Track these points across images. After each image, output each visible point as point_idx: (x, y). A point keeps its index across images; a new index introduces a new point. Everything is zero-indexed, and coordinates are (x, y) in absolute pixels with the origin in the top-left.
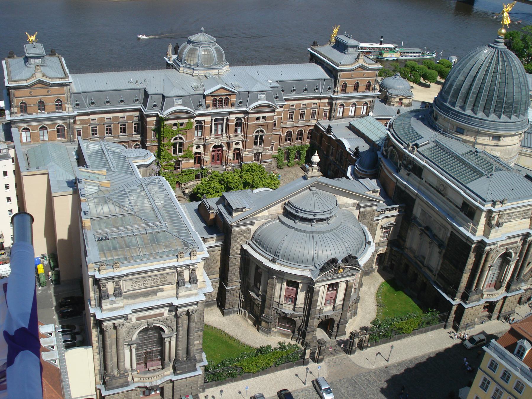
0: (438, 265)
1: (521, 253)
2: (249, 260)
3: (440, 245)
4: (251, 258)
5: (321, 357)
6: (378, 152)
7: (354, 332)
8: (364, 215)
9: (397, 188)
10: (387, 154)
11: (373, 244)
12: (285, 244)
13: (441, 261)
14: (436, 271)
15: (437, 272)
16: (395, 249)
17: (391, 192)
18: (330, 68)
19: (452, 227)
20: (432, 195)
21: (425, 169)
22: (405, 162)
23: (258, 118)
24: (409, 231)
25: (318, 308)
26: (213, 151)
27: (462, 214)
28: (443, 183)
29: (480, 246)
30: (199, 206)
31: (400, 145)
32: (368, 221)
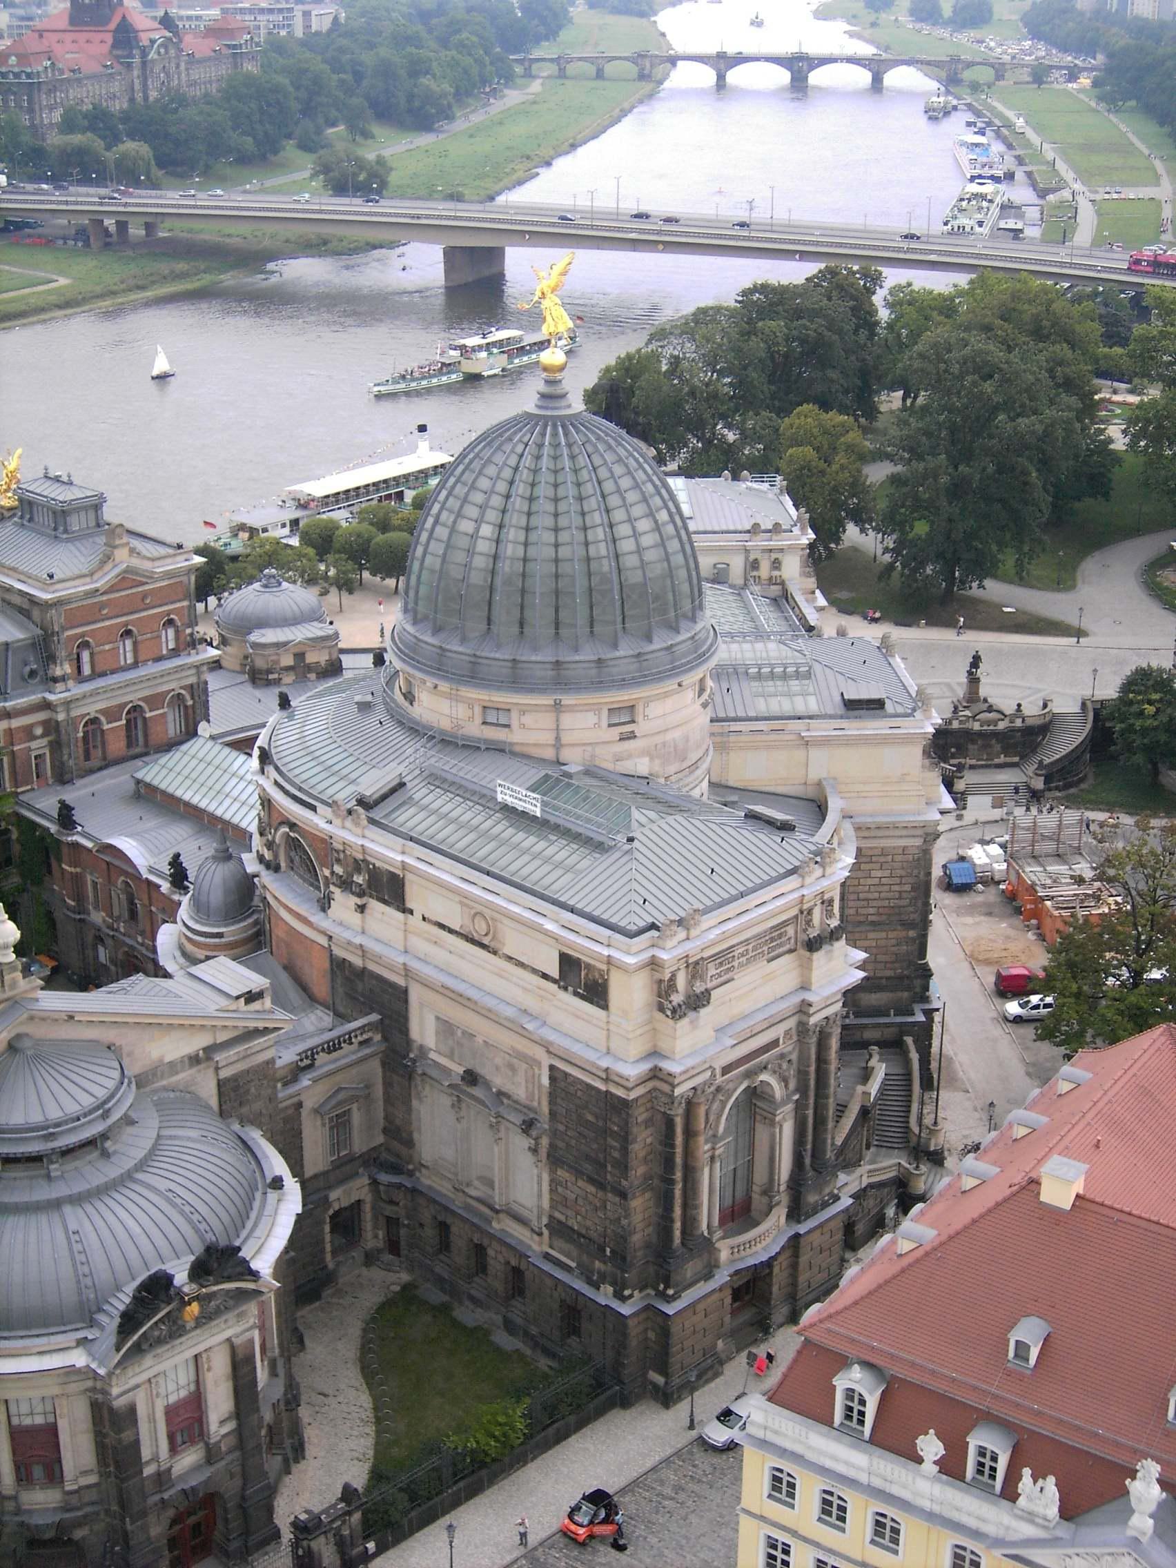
0: (540, 1196)
1: (802, 1074)
3: (528, 1126)
6: (245, 856)
7: (303, 1517)
9: (339, 966)
10: (276, 856)
11: (292, 1187)
13: (546, 1177)
14: (539, 1218)
15: (545, 1221)
16: (384, 1178)
17: (321, 987)
18: (17, 600)
19: (549, 1052)
21: (409, 877)
22: (338, 869)
24: (415, 1103)
25: (148, 1471)
27: (568, 999)
28: (480, 908)
29: (655, 1089)
31: (308, 814)
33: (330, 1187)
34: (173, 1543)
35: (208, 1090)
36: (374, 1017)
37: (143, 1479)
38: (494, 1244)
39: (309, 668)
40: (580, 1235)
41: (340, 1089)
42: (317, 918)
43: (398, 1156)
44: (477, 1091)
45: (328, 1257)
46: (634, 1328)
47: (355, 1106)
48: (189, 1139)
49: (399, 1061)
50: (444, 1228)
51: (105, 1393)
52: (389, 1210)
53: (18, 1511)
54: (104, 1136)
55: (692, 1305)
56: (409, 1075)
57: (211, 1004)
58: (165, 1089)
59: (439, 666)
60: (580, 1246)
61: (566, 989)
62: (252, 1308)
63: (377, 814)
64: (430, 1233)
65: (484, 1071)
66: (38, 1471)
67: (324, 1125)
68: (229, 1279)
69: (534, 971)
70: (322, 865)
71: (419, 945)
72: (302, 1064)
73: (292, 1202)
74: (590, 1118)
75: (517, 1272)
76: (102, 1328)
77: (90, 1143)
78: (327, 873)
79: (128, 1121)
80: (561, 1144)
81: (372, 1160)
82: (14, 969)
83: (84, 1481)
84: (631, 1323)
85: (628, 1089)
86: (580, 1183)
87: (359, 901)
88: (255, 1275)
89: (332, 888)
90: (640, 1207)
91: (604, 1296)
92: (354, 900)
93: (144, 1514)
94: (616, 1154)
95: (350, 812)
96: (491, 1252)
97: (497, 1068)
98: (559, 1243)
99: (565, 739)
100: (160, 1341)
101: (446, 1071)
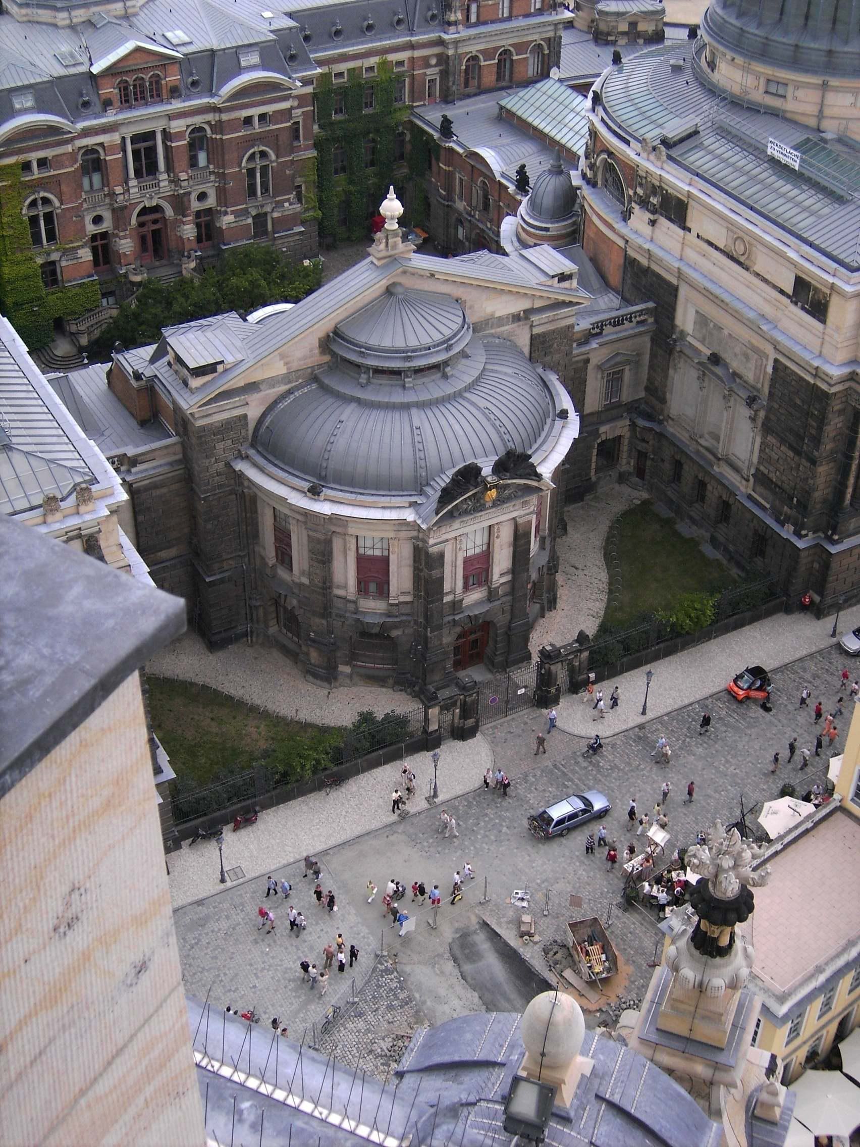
0: (752, 452)
2: (254, 499)
3: (751, 401)
4: (259, 494)
5: (470, 722)
6: (573, 173)
7: (548, 648)
8: (543, 343)
9: (630, 263)
10: (595, 175)
11: (574, 418)
12: (341, 443)
13: (758, 440)
14: (749, 468)
15: (753, 471)
16: (641, 422)
17: (615, 277)
19: (775, 348)
20: (715, 270)
21: (692, 203)
22: (640, 191)
23: (248, 121)
24: (671, 372)
26: (141, 225)
27: (796, 311)
28: (741, 234)
29: (850, 388)
30: (109, 374)
32: (557, 357)
33: (602, 423)
34: (457, 650)
35: (523, 340)
36: (651, 305)
37: (443, 604)
38: (713, 482)
39: (639, 35)
40: (776, 485)
41: (617, 354)
42: (619, 226)
43: (653, 407)
44: (718, 370)
45: (593, 472)
46: (804, 559)
47: (627, 368)
48: (505, 374)
49: (664, 339)
50: (678, 465)
51: (425, 542)
52: (641, 446)
53: (356, 612)
54: (446, 363)
55: (850, 550)
56: (670, 351)
57: (534, 279)
58: (493, 336)
59: (738, 44)
60: (775, 493)
61: (796, 304)
62: (534, 499)
63: (674, 153)
64: (667, 466)
65: (727, 356)
66: (372, 587)
67: (603, 378)
68: (521, 477)
69: (775, 287)
70: (629, 186)
71: (691, 255)
72: (594, 332)
73: (571, 431)
74: (798, 402)
75: (726, 506)
76: (428, 497)
77: (435, 367)
78: (631, 192)
79: (463, 354)
80: (772, 417)
81: (633, 408)
82: (396, 235)
83: (402, 599)
84: (803, 554)
85: (831, 385)
86: (783, 448)
87: (652, 217)
88: (539, 477)
89: (633, 205)
90: (824, 472)
91: (787, 532)
92: (648, 216)
93: (440, 627)
94: (813, 432)
95: (654, 149)
96: (709, 487)
97: (736, 355)
98: (760, 489)
99: (827, 112)
100: (467, 512)
101: (697, 351)
